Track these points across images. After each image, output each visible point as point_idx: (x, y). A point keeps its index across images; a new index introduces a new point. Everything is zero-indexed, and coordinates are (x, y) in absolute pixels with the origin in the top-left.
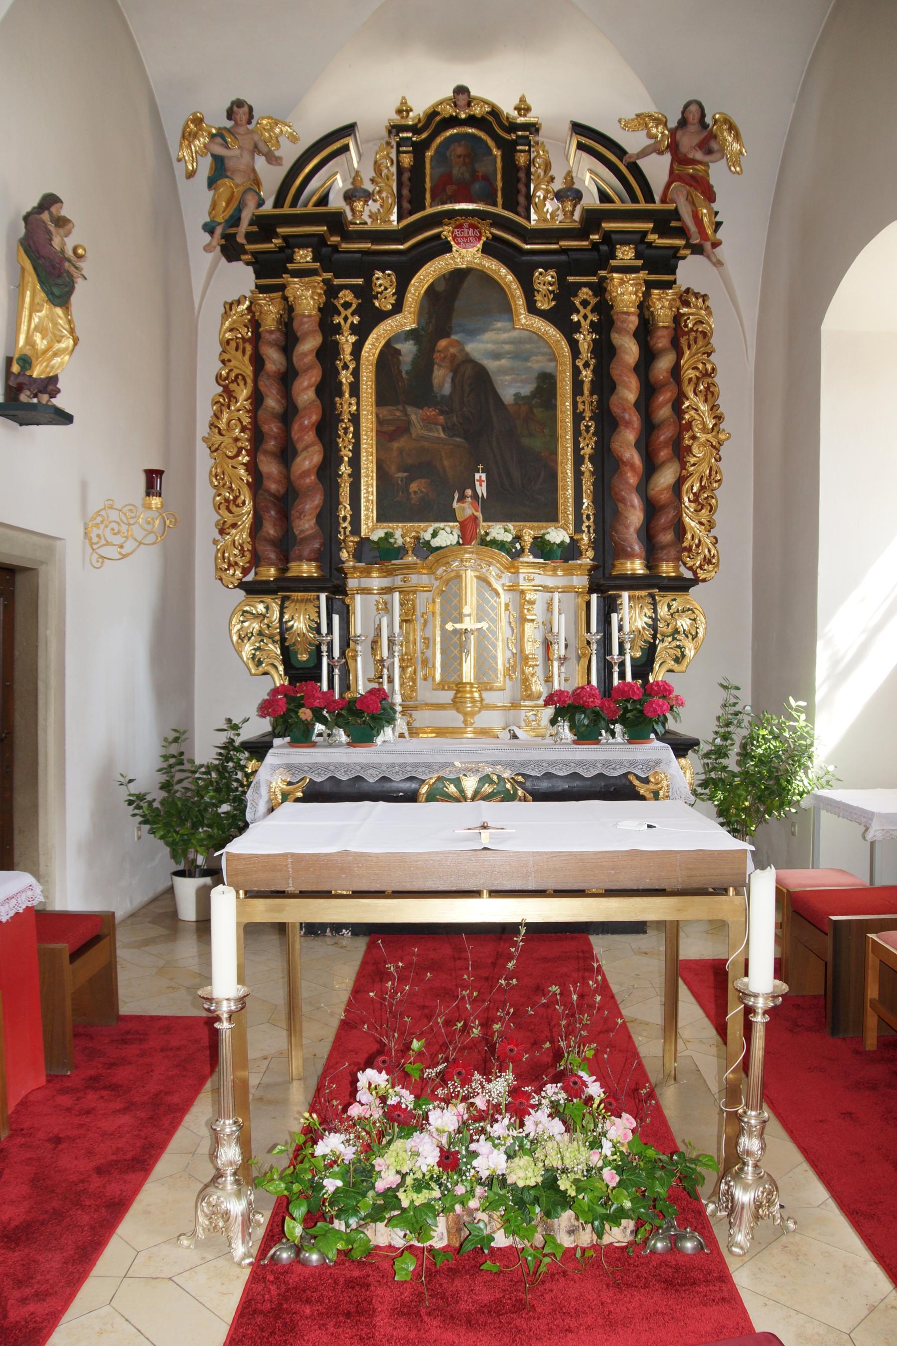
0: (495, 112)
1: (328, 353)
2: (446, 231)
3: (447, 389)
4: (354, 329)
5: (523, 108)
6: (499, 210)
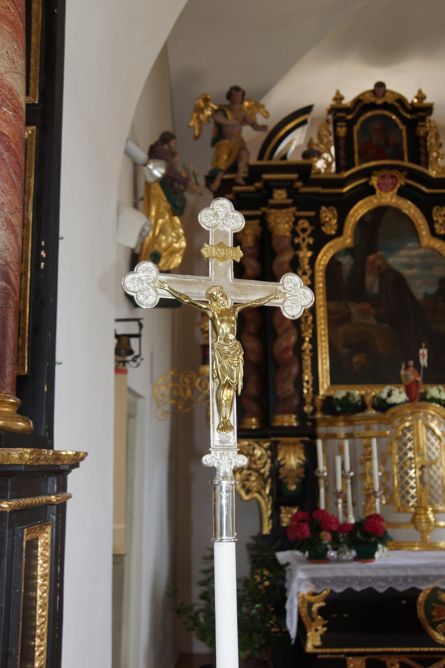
0: (401, 100)
3: (376, 289)
4: (310, 247)
5: (421, 96)
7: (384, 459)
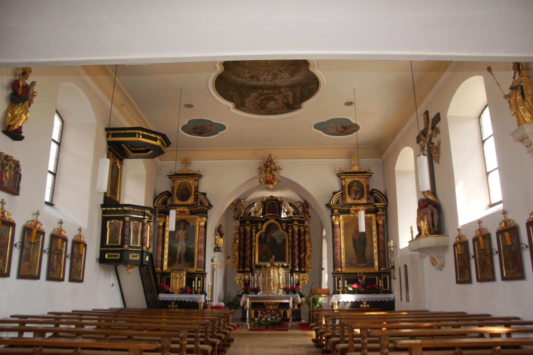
1: (251, 236)
2: (269, 217)
6: (277, 215)
7: (263, 276)
